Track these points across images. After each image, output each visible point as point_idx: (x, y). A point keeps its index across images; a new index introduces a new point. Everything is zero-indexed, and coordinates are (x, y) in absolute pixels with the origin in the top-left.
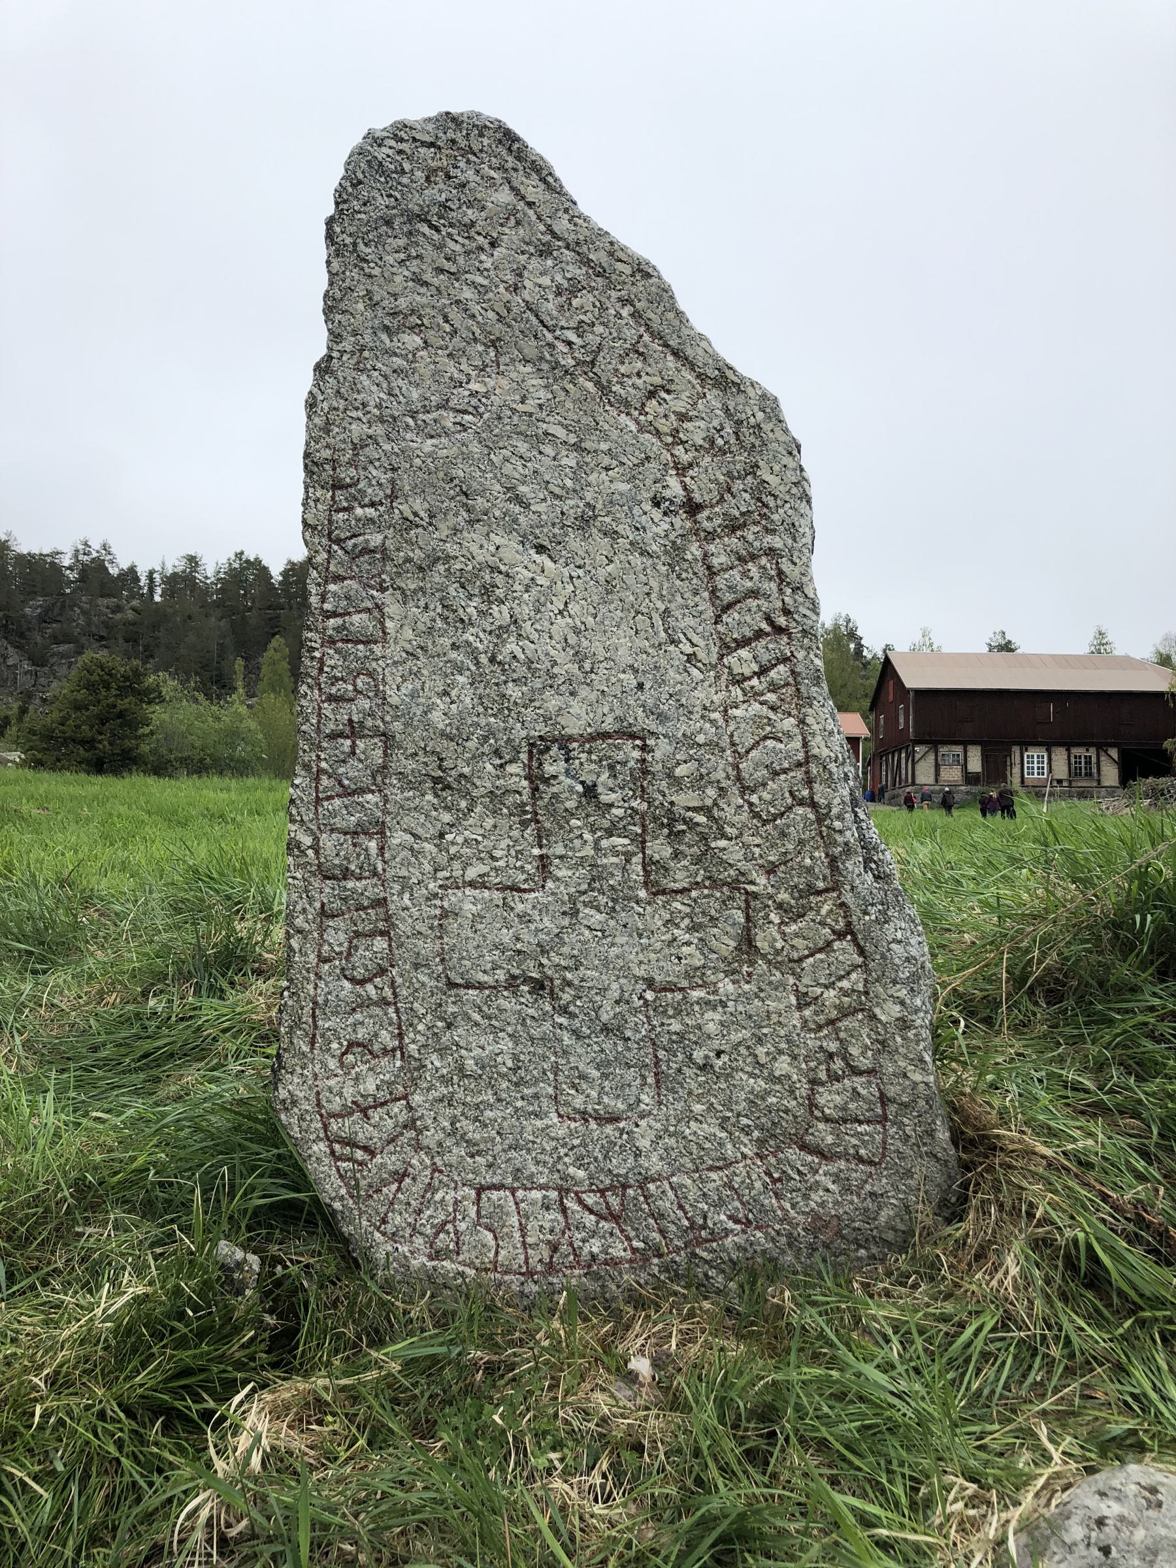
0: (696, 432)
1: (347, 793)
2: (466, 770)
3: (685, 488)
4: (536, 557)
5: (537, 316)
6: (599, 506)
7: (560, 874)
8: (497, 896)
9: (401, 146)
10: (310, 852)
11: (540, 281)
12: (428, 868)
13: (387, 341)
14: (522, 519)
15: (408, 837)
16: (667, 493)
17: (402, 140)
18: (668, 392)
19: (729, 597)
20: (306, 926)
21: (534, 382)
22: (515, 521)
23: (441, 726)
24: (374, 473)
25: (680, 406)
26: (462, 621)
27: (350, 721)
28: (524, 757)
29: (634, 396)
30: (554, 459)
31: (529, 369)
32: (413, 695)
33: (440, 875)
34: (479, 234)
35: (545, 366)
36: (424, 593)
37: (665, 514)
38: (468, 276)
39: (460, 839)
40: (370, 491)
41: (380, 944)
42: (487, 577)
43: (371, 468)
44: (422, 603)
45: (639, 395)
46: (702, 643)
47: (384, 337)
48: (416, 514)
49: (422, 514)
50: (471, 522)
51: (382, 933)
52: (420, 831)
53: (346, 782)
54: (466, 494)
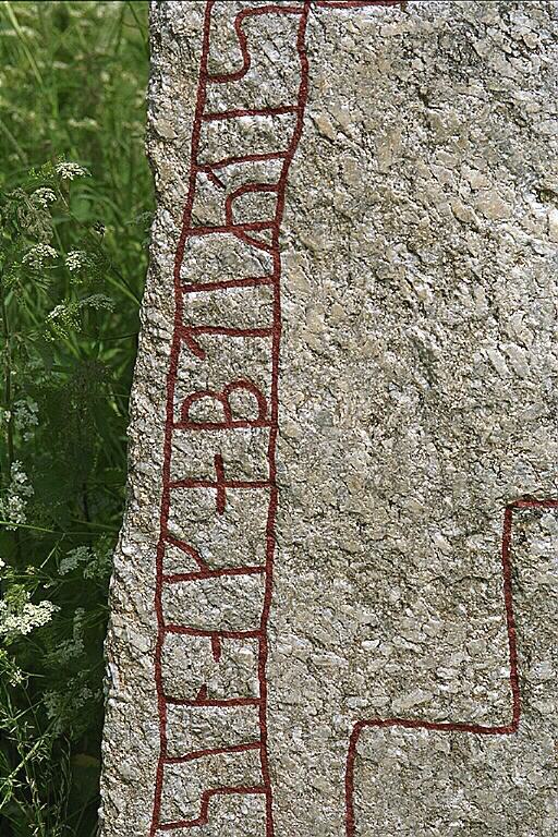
1: (207, 571)
2: (402, 543)
7: (541, 706)
8: (442, 740)
10: (147, 661)
12: (334, 691)
14: (516, 145)
15: (302, 643)
20: (137, 774)
23: (365, 472)
24: (273, 56)
26: (408, 305)
27: (219, 460)
28: (497, 527)
32: (322, 422)
33: (351, 702)
36: (347, 257)
39: (387, 650)
40: (265, 86)
41: (254, 803)
43: (267, 47)
44: (342, 273)
48: (340, 129)
49: (352, 129)
50: (430, 145)
51: (257, 789)
52: (323, 635)
53: (208, 555)
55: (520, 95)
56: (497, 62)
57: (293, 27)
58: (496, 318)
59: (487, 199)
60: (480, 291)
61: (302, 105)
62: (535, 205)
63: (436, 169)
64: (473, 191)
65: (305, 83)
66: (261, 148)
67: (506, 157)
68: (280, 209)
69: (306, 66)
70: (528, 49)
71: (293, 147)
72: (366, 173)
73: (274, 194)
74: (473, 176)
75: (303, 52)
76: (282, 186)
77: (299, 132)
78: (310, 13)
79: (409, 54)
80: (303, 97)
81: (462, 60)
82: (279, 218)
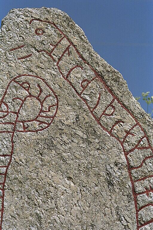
0: (133, 140)
3: (127, 158)
4: (68, 182)
6: (94, 163)
9: (26, 18)
11: (77, 75)
13: (15, 92)
14: (63, 166)
16: (121, 161)
17: (27, 16)
18: (123, 122)
19: (141, 204)
21: (71, 113)
22: (60, 166)
24: (5, 142)
25: (127, 128)
26: (35, 205)
29: (111, 123)
30: (78, 143)
31: (69, 108)
34: (54, 55)
35: (76, 108)
36: (21, 192)
37: (119, 169)
38: (49, 70)
40: (3, 150)
42: (47, 188)
44: (20, 196)
45: (112, 122)
46: (130, 221)
47: (14, 90)
48: (21, 160)
49: (23, 161)
50: (42, 165)
54: (41, 154)
55: (64, 154)
56: (59, 146)
57: (10, 136)
58: (57, 208)
59: (55, 179)
60: (53, 201)
61: (12, 154)
62: (67, 181)
63: (44, 170)
64: (52, 177)
65: (13, 149)
66: (1, 165)
67: (60, 169)
68: (5, 180)
69: (13, 145)
70: (66, 144)
71: (9, 164)
72: (26, 171)
73: (4, 176)
74: (52, 173)
75: (13, 142)
76: (6, 174)
77: (10, 161)
78: (15, 133)
79: (38, 143)
80: (12, 153)
81: (51, 146)
82: (5, 182)
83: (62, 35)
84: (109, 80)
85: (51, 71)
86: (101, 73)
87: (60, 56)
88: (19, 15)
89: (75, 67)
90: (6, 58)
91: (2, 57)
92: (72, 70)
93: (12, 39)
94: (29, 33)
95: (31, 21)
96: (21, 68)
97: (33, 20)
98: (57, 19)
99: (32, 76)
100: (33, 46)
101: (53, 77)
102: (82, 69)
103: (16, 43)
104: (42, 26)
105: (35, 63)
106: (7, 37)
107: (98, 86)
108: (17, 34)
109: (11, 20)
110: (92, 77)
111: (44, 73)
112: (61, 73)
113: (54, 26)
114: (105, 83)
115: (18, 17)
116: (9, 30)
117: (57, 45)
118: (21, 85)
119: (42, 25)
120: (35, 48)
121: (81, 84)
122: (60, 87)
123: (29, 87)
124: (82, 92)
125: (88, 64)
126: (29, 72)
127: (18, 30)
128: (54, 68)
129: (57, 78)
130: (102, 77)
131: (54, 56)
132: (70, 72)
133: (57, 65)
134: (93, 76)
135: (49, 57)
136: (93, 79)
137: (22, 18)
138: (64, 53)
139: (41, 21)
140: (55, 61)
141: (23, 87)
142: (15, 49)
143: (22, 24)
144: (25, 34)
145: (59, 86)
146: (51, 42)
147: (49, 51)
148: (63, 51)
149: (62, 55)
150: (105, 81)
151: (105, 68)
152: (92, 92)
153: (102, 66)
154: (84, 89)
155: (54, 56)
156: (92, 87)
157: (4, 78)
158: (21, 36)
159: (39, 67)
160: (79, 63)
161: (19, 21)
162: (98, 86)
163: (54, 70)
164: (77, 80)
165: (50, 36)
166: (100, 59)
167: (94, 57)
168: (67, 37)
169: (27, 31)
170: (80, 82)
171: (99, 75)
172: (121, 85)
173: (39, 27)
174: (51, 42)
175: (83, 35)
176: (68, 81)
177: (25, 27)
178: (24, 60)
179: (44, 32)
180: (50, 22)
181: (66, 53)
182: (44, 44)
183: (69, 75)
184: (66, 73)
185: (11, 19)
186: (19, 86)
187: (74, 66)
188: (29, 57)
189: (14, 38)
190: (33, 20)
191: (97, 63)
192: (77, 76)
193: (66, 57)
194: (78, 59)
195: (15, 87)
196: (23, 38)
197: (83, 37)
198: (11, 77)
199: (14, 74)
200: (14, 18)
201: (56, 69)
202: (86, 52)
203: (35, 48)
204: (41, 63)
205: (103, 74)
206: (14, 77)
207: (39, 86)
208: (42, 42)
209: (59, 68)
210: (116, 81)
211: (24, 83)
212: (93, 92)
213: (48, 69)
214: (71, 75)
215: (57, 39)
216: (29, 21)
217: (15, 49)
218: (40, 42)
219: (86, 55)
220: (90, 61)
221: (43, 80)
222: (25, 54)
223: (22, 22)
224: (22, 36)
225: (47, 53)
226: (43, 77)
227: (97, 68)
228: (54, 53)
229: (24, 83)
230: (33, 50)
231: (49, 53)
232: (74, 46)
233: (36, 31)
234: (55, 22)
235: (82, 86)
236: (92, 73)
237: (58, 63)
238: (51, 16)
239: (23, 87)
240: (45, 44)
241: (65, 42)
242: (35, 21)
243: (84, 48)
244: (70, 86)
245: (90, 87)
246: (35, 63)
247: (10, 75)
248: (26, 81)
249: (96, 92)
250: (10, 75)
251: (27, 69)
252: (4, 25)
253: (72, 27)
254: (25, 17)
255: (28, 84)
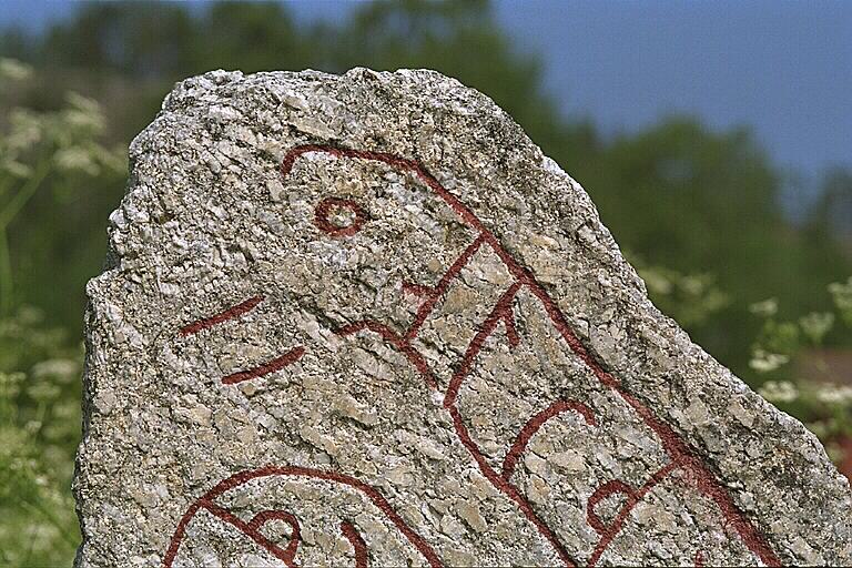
5: (553, 537)
9: (259, 142)
11: (561, 459)
17: (267, 130)
34: (429, 345)
38: (401, 434)
83: (472, 230)
84: (745, 476)
85: (411, 438)
86: (700, 439)
87: (463, 350)
88: (222, 125)
89: (553, 411)
90: (160, 376)
91: (132, 371)
92: (531, 427)
93: (186, 264)
94: (283, 226)
95: (290, 159)
96: (246, 434)
97: (299, 149)
98: (439, 138)
99: (309, 472)
100: (306, 299)
101: (425, 472)
102: (589, 418)
103: (209, 287)
104: (354, 186)
105: (325, 397)
106: (159, 259)
107: (687, 518)
108: (213, 235)
109: (176, 159)
110: (647, 467)
111: (376, 452)
112: (473, 447)
113: (422, 181)
114: (725, 498)
115: (216, 137)
116: (166, 214)
117: (443, 287)
118: (250, 530)
119: (351, 177)
120: (319, 312)
121: (590, 512)
122: (472, 531)
123: (297, 536)
124: (596, 556)
125: (624, 390)
126: (290, 450)
127: (218, 211)
128: (433, 421)
129: (452, 479)
130: (707, 465)
131: (426, 353)
132: (520, 442)
133: (447, 404)
134: (656, 462)
135: (402, 359)
136: (657, 478)
137: (239, 143)
138: (484, 329)
139: (349, 152)
140: (432, 378)
141: (262, 541)
142: (205, 323)
143: (240, 177)
144: (258, 231)
145: (465, 523)
146: (410, 271)
147: (398, 324)
148: (480, 320)
149: (472, 344)
150: (725, 486)
151: (721, 407)
152: (654, 555)
153: (702, 397)
154: (608, 537)
155: (426, 353)
156: (653, 525)
157: (151, 496)
158: (238, 249)
159: (345, 420)
160: (571, 384)
161: (222, 158)
162: (687, 518)
163: (432, 433)
164: (567, 487)
165: (400, 237)
166: (694, 360)
167: (656, 347)
168: (500, 236)
169: (269, 217)
170: (584, 497)
171: (688, 452)
172: (820, 504)
173: (335, 188)
174: (410, 271)
175: (590, 223)
176: (514, 492)
177: (258, 190)
178: (258, 383)
179: (365, 215)
180: (401, 159)
181: (494, 331)
182: (368, 287)
183: (517, 456)
184: (497, 450)
185: (175, 154)
186: (237, 532)
187: (546, 404)
188: (290, 367)
189: (199, 262)
190: (299, 149)
191: (678, 386)
192: (563, 462)
193: (498, 357)
194: (567, 361)
195: (217, 542)
196: (249, 258)
197: (587, 233)
198: (192, 488)
199: (209, 468)
200: (192, 142)
201: (442, 424)
202: (609, 323)
203: (319, 312)
204: (356, 396)
205: (710, 444)
206: (208, 486)
207: (349, 527)
208: (355, 279)
209: (460, 422)
210: (787, 482)
211: (262, 517)
212: (660, 550)
213: (399, 427)
214: (531, 460)
215: (442, 256)
216: (281, 156)
217: (205, 323)
218: (347, 277)
219: (608, 341)
220: (631, 369)
221: (373, 492)
222: (263, 350)
223: (237, 163)
224: (243, 245)
225: (388, 336)
226: (371, 477)
227: (676, 413)
228: (428, 332)
229: (262, 517)
230: (311, 325)
231: (401, 337)
232: (541, 289)
233: (321, 214)
234: (425, 159)
235: (594, 520)
236: (648, 444)
237: (451, 394)
238: (405, 122)
239: (262, 541)
240: (376, 284)
241: (486, 269)
242: (310, 155)
243: (598, 297)
244: (525, 525)
245: (641, 526)
246: (325, 397)
247: (183, 473)
248: (277, 504)
249: (679, 553)
250: (183, 473)
251: (280, 437)
252: (138, 184)
253: (526, 182)
254: (256, 134)
255: (291, 519)
